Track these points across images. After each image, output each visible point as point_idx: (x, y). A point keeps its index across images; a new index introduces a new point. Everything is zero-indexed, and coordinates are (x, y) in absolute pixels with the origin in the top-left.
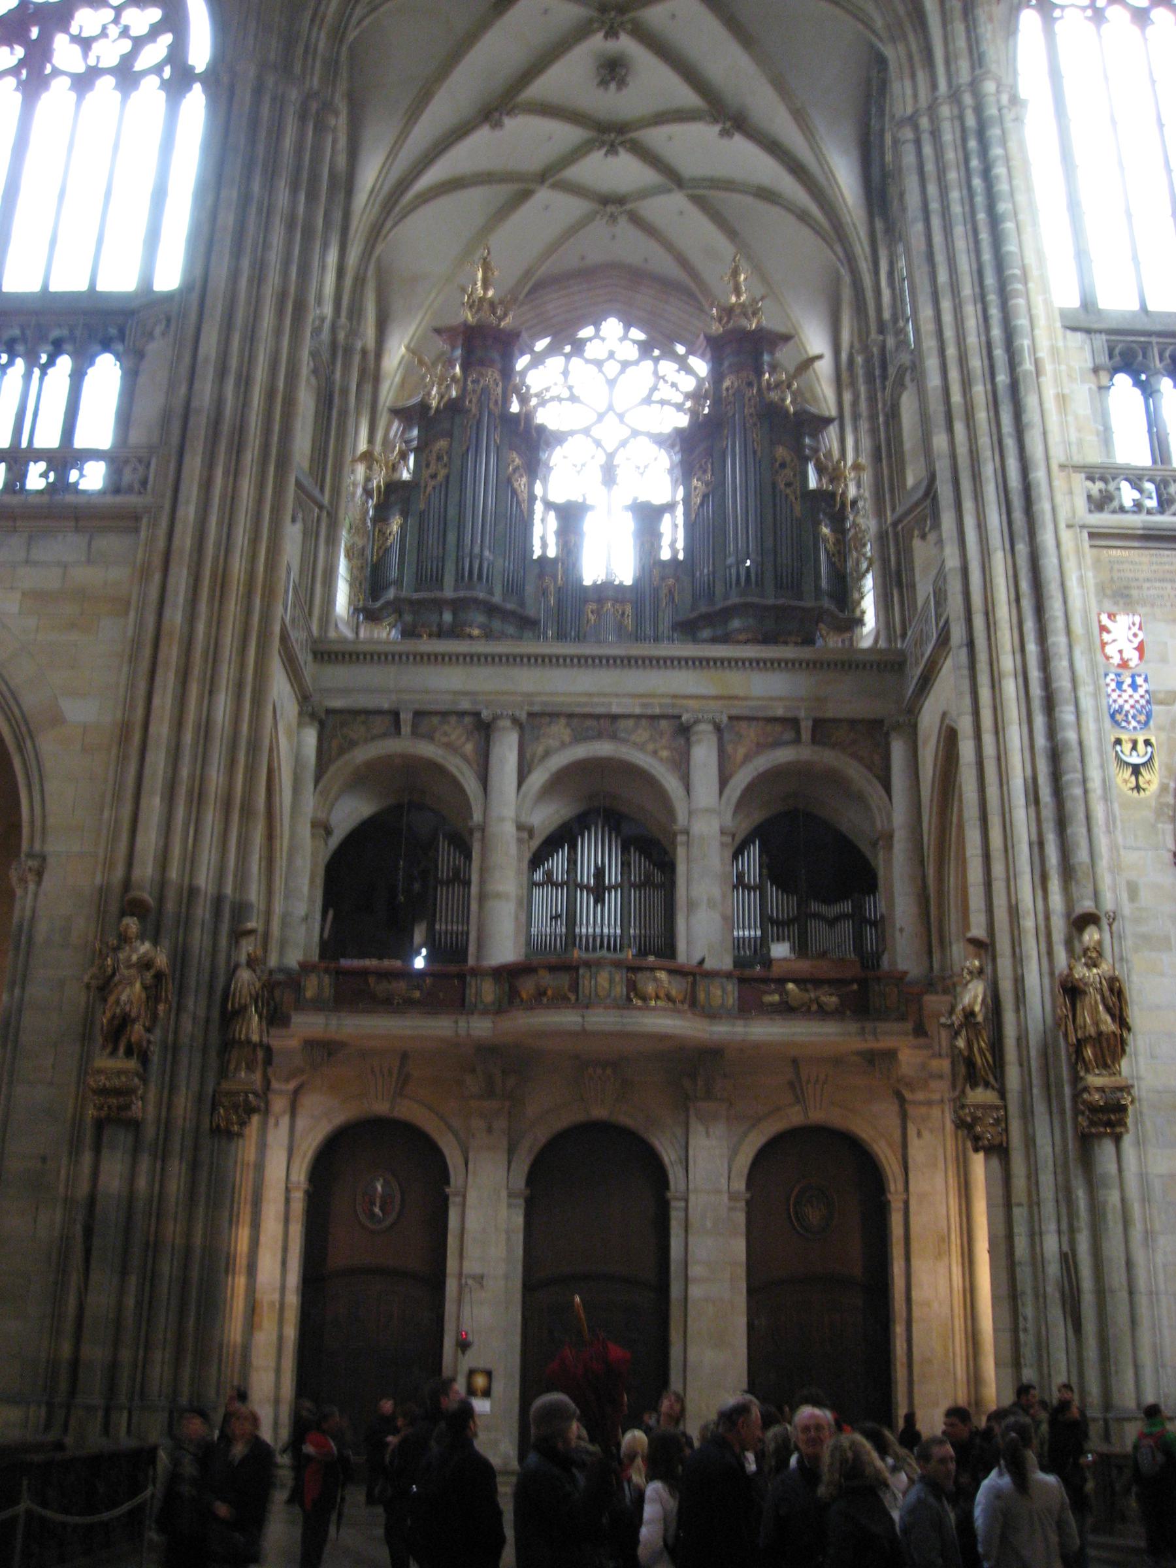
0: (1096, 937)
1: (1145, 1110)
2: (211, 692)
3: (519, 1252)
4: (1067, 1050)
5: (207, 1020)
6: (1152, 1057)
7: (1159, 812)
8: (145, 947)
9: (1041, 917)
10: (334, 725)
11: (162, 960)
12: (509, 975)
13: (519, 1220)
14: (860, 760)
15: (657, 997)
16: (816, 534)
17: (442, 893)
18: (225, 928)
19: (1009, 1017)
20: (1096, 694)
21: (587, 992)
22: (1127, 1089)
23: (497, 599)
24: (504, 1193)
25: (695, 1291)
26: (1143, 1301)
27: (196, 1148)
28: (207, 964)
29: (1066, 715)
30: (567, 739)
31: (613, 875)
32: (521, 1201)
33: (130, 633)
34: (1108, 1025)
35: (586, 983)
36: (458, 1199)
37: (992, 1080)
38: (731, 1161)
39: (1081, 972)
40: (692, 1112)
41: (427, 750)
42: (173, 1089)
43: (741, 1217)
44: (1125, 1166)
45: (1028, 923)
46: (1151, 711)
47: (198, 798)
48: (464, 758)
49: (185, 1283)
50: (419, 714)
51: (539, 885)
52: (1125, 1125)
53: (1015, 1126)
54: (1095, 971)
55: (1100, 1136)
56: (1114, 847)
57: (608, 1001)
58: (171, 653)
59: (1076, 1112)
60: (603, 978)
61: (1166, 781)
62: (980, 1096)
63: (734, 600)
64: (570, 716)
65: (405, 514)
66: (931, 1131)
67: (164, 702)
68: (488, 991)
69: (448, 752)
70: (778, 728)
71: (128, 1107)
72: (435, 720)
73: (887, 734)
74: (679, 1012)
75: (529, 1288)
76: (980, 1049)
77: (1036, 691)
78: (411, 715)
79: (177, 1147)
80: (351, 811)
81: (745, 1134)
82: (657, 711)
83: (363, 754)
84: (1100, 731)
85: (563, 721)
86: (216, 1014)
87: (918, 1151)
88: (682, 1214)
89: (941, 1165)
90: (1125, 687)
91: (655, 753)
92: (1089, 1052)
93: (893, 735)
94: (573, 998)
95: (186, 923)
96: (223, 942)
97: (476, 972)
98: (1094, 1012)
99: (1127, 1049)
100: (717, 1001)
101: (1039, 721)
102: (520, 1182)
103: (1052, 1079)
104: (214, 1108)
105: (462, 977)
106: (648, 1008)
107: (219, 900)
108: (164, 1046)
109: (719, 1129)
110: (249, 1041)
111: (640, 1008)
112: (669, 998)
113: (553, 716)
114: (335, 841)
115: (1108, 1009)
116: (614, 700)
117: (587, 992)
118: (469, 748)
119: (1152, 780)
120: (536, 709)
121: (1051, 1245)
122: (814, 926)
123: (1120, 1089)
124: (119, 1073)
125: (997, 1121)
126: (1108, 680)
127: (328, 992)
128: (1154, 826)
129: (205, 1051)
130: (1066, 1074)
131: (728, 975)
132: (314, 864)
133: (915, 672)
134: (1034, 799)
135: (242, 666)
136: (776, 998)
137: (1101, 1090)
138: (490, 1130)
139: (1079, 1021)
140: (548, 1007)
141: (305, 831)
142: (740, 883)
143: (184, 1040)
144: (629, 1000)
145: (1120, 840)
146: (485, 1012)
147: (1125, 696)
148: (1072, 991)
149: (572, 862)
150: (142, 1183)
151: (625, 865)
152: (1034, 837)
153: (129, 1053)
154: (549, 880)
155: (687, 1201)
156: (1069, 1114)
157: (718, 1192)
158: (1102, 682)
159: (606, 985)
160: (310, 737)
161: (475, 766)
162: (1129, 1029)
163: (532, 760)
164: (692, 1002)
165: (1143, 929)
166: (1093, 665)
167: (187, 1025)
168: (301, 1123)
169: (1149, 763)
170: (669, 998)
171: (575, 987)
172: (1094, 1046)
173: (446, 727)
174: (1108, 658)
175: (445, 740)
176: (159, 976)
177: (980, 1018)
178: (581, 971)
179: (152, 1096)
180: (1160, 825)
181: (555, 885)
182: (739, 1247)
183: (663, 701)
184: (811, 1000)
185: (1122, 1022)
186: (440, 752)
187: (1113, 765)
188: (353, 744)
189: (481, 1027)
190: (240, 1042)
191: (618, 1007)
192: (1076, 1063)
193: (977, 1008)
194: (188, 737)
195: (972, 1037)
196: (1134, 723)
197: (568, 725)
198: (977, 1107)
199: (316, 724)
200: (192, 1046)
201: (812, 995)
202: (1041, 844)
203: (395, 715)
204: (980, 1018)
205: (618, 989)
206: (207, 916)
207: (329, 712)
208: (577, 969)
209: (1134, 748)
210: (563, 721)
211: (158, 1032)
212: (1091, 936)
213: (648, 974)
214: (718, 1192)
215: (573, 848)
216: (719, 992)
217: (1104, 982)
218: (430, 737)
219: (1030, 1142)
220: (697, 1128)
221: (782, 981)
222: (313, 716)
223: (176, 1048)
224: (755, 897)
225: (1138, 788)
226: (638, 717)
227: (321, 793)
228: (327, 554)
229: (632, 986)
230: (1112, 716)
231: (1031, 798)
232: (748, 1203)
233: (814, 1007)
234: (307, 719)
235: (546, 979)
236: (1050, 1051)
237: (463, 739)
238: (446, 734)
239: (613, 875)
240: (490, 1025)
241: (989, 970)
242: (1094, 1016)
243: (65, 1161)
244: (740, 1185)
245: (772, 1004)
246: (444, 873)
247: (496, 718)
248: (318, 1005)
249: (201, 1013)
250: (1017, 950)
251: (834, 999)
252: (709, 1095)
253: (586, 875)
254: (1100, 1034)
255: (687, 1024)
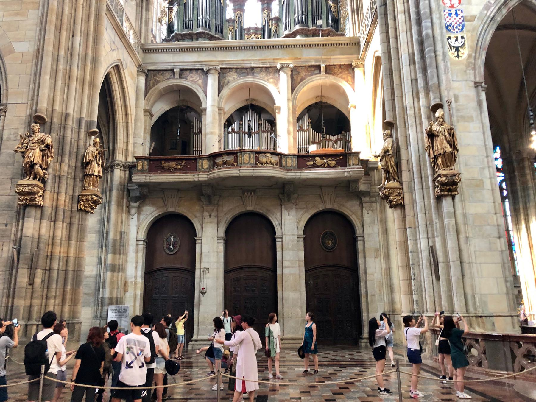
0: (442, 113)
1: (464, 187)
2: (73, 36)
3: (222, 260)
4: (430, 161)
5: (76, 167)
6: (466, 165)
7: (468, 66)
8: (41, 135)
9: (416, 109)
10: (151, 75)
11: (49, 141)
12: (213, 157)
13: (221, 247)
14: (344, 78)
15: (267, 163)
16: (327, 5)
17: (195, 137)
18: (83, 130)
19: (403, 152)
20: (440, 18)
21: (241, 162)
22: (458, 175)
23: (213, 33)
24: (216, 238)
25: (286, 271)
26: (466, 266)
27: (71, 217)
28: (76, 145)
29: (426, 23)
30: (236, 77)
31: (255, 128)
32: (222, 241)
33: (40, 15)
34: (449, 149)
35: (240, 159)
36: (200, 241)
37: (396, 178)
38: (298, 223)
39: (435, 127)
40: (283, 207)
41: (185, 83)
42: (58, 193)
43: (302, 243)
44: (457, 209)
45: (410, 112)
46: (464, 24)
47: (68, 77)
48: (198, 85)
49: (66, 271)
50: (181, 70)
51: (229, 133)
52: (456, 190)
53: (406, 196)
54: (442, 127)
55: (445, 196)
56: (448, 80)
57: (248, 165)
58: (53, 18)
59: (435, 187)
60: (246, 157)
61: (471, 53)
62: (393, 184)
63: (297, 27)
64: (237, 68)
65: (179, 5)
66: (372, 211)
67: (50, 36)
68: (205, 164)
69: (191, 82)
70: (313, 69)
71: (33, 200)
72: (188, 72)
73: (353, 69)
74: (275, 168)
75: (227, 272)
76: (391, 164)
77: (413, 16)
78: (178, 70)
79: (61, 217)
80: (161, 108)
81: (303, 214)
82: (268, 65)
83: (162, 85)
84: (442, 33)
85: (234, 70)
86: (79, 164)
87: (367, 218)
88: (280, 243)
89: (376, 223)
90: (452, 15)
91: (268, 80)
92: (440, 161)
93: (356, 69)
94: (236, 164)
95: (64, 128)
96: (82, 136)
97: (201, 158)
98: (442, 144)
99: (457, 159)
100: (289, 164)
101: (415, 29)
102: (222, 234)
103: (423, 175)
104: (79, 202)
105: (196, 159)
106: (263, 167)
107: (80, 120)
108: (55, 177)
109: (293, 212)
110: (93, 174)
111: (260, 167)
112: (272, 164)
113: (231, 69)
114: (155, 119)
115: (448, 142)
116: (252, 62)
117: (241, 162)
118: (200, 82)
119: (465, 53)
120: (224, 66)
121: (423, 244)
122: (328, 143)
123: (455, 175)
124: (29, 185)
125: (399, 194)
126: (445, 13)
127: (146, 167)
128: (465, 71)
129: (75, 179)
130: (429, 172)
131: (294, 155)
132: (145, 126)
133: (362, 44)
134: (412, 61)
135: (88, 27)
136: (312, 163)
137: (445, 175)
138: (210, 216)
139: (436, 148)
140: (226, 168)
141: (141, 113)
142: (301, 129)
143: (64, 174)
144: (256, 164)
145: (450, 77)
146: (205, 172)
147: (453, 19)
148: (432, 135)
149: (241, 125)
150: (44, 231)
151: (260, 125)
152: (413, 77)
153: (35, 178)
154: (233, 131)
155: (282, 238)
156: (431, 188)
157: (293, 235)
158: (442, 13)
159: (248, 159)
160: (142, 80)
161: (203, 88)
162: (458, 151)
163: (223, 86)
164: (281, 165)
165: (460, 114)
166: (439, 6)
167: (65, 168)
168: (142, 217)
169: (463, 46)
170: (272, 164)
171: (236, 160)
172: (442, 158)
173: (191, 75)
174: (445, 4)
175: (191, 79)
176: (48, 146)
177: (391, 153)
178: (238, 154)
179: (48, 195)
180: (468, 71)
181: (235, 133)
182: (302, 255)
183: (270, 61)
184: (325, 163)
185: (454, 146)
186: (189, 83)
187: (447, 48)
188: (158, 82)
189: (203, 177)
190: (90, 175)
191: (252, 167)
192: (434, 166)
193: (390, 149)
194: (62, 53)
195: (388, 160)
196: (456, 30)
197: (236, 72)
198: (391, 189)
199: (144, 75)
200: (68, 177)
201: (325, 161)
202: (416, 80)
203: (173, 70)
204: (391, 153)
205: (252, 160)
206: (74, 126)
207: (149, 71)
208: (237, 153)
209: (456, 40)
210: (234, 70)
211: (50, 170)
212: (439, 113)
213: (263, 154)
214: (293, 235)
215: (241, 120)
216: (290, 161)
217: (446, 130)
218: (186, 78)
219: (413, 202)
220: (285, 213)
221: (314, 156)
222: (142, 71)
223: (60, 177)
224: (306, 134)
225: (458, 56)
226: (262, 68)
227: (147, 100)
228: (146, 14)
229: (257, 159)
230: (447, 28)
231: (412, 61)
232: (305, 239)
233: (326, 165)
234: (140, 73)
235: (226, 158)
236: (422, 164)
237: (198, 78)
238: (192, 77)
239: (255, 128)
240: (206, 176)
241: (394, 135)
242: (442, 145)
243: (14, 224)
244: (301, 232)
245: (310, 165)
246: (196, 130)
247: (208, 70)
248: (142, 172)
249: (74, 165)
250: (407, 124)
251: (334, 162)
252: (289, 200)
253: (246, 129)
254: (445, 152)
255: (277, 172)
